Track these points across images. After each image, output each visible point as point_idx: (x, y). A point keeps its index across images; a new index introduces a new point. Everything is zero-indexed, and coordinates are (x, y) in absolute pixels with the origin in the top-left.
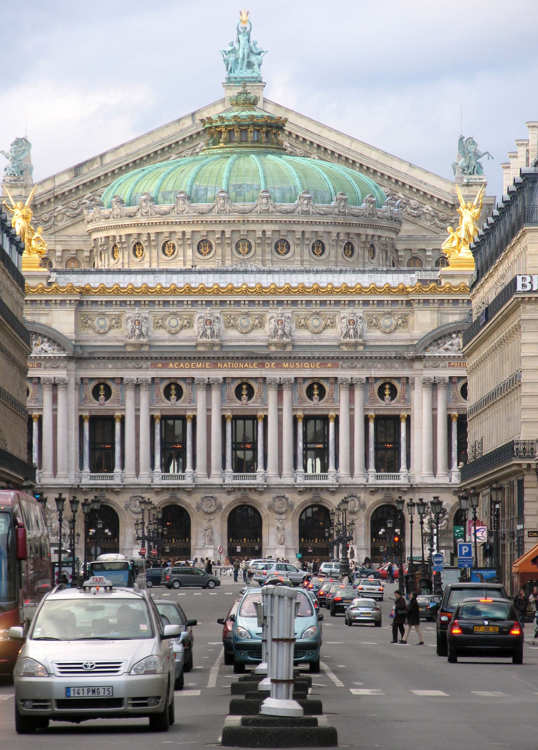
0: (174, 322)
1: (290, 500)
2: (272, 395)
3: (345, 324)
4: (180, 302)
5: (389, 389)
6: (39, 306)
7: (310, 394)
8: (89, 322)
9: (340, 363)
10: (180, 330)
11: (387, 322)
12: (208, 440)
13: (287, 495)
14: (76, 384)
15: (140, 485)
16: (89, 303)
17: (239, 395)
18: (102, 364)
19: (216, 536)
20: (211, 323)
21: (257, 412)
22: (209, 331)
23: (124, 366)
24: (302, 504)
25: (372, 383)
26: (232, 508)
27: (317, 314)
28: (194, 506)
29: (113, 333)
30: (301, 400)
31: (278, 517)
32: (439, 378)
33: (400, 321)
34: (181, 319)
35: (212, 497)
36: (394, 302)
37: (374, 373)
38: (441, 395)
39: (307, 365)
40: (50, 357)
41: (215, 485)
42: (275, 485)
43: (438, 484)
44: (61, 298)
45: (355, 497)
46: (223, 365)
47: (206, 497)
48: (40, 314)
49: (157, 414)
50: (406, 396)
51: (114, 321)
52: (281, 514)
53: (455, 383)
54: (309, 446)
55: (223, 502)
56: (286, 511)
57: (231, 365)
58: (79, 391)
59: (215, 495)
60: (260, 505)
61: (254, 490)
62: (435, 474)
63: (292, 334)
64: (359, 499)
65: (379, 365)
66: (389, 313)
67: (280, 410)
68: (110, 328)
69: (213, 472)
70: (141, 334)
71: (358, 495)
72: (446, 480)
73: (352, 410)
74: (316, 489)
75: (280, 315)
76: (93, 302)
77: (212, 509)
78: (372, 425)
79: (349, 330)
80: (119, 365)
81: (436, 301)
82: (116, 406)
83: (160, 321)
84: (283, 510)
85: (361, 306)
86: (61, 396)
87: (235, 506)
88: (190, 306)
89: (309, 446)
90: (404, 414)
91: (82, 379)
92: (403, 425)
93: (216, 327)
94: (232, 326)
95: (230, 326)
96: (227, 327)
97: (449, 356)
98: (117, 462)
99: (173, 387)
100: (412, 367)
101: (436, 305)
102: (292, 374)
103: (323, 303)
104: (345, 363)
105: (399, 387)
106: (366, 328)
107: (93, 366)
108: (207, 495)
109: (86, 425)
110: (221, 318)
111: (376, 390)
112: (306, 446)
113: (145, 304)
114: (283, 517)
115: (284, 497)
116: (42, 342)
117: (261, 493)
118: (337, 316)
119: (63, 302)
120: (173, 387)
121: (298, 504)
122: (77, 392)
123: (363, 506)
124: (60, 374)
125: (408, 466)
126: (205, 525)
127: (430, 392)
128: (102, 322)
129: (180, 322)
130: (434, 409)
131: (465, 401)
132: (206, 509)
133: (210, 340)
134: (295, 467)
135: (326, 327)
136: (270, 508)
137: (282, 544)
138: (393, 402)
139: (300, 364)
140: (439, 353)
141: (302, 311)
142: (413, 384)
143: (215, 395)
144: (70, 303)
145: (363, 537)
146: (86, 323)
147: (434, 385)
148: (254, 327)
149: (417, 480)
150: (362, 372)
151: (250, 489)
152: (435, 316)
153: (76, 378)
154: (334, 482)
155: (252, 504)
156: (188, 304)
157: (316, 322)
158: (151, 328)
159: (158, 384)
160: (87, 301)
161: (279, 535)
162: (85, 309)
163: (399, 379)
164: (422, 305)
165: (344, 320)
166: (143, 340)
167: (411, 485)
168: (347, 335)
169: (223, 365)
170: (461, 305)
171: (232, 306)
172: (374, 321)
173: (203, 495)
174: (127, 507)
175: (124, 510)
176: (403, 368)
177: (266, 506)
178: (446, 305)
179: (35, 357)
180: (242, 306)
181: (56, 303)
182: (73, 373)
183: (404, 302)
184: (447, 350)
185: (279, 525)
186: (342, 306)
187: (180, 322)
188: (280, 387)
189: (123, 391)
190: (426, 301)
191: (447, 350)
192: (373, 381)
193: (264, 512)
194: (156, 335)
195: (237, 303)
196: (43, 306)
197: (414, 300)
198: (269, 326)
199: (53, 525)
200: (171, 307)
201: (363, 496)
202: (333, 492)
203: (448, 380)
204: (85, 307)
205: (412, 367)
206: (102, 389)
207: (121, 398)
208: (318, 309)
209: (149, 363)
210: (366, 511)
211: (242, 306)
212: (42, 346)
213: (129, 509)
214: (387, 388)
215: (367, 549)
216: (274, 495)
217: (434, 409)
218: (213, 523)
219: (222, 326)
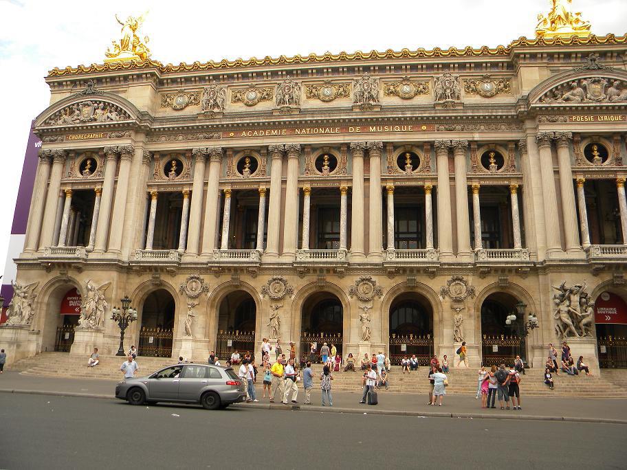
0: (252, 95)
1: (377, 284)
2: (358, 162)
3: (440, 86)
4: (260, 74)
5: (494, 158)
6: (118, 84)
7: (402, 165)
8: (168, 100)
9: (436, 126)
10: (259, 102)
11: (487, 86)
12: (284, 218)
13: (374, 278)
14: (144, 157)
15: (198, 264)
16: (169, 81)
17: (319, 166)
18: (172, 137)
19: (285, 329)
20: (289, 89)
21: (340, 184)
22: (287, 96)
23: (195, 137)
24: (393, 290)
25: (474, 151)
26: (306, 295)
27: (406, 79)
28: (259, 290)
29: (188, 109)
30: (390, 169)
31: (362, 305)
32: (560, 134)
33: (502, 85)
34: (260, 92)
35: (281, 280)
36: (495, 65)
37: (477, 137)
38: (564, 154)
39: (397, 128)
40: (114, 125)
41: (285, 264)
42: (359, 265)
43: (572, 260)
44: (137, 73)
45: (461, 280)
46: (301, 132)
47: (274, 280)
48: (118, 92)
49: (227, 188)
50: (515, 164)
51: (192, 98)
52: (366, 301)
53: (577, 143)
54: (401, 236)
55: (295, 285)
56: (373, 297)
57: (310, 131)
58: (150, 167)
59: (285, 278)
60: (340, 290)
61: (332, 271)
62: (565, 248)
63: (380, 100)
64: (466, 283)
65: (482, 127)
66: (488, 77)
67: (367, 180)
68: (187, 105)
69: (285, 250)
70: (216, 105)
71: (465, 278)
72: (583, 256)
73: (452, 179)
74: (412, 269)
75: (367, 78)
76: (174, 81)
77: (280, 295)
78: (476, 197)
79: (445, 90)
80: (190, 137)
81: (545, 55)
82: (184, 181)
83: (238, 95)
84: (370, 295)
85: (457, 71)
86: (124, 165)
87: (310, 292)
88: (270, 79)
89: (401, 236)
90: (514, 184)
91: (153, 154)
92: (514, 197)
93: (296, 93)
94: (314, 96)
95: (312, 95)
96: (308, 98)
97: (571, 107)
98: (182, 242)
99: (248, 160)
100: (522, 128)
101: (544, 61)
102: (381, 139)
103: (414, 67)
104: (441, 124)
105: (506, 155)
106: (463, 93)
107: (163, 139)
108: (275, 277)
109: (154, 202)
110: (302, 89)
111: (479, 158)
112: (398, 236)
113: (224, 79)
114: (369, 305)
115: (369, 280)
116: (111, 112)
117: (341, 275)
118: (430, 82)
119: (139, 76)
120: (248, 160)
121: (388, 289)
122: (145, 166)
123: (471, 292)
124: (124, 143)
125: (524, 244)
126: (271, 312)
127: (549, 150)
128: (180, 100)
129: (259, 95)
130: (557, 172)
131: (591, 164)
132: (274, 295)
133: (288, 105)
134: (385, 246)
135: (418, 93)
136: (352, 293)
137: (366, 340)
138: (500, 170)
139: (389, 128)
140: (559, 103)
141: (390, 76)
142: (525, 146)
143: (293, 163)
144: (147, 78)
145: (473, 332)
146: (166, 101)
147: (554, 143)
148: (338, 96)
149: (541, 259)
150: (462, 135)
151: (328, 270)
152: (546, 74)
153: (144, 152)
154: (435, 260)
155: (331, 290)
156: (267, 76)
157: (406, 89)
158: (229, 102)
159: (230, 156)
160: (167, 79)
161: (364, 329)
162: (166, 88)
163: (504, 144)
164: (527, 61)
165: (439, 82)
166: (216, 110)
167: (534, 263)
168: (443, 96)
169: (301, 132)
170: (573, 61)
171: (315, 76)
172: (472, 85)
173: (270, 278)
174: (183, 290)
175: (179, 294)
176: (512, 131)
177: (347, 291)
178: (556, 61)
179: (100, 126)
180: (325, 76)
181: (133, 79)
182: (141, 144)
183: (505, 64)
184: (567, 100)
185: (364, 315)
186: (436, 71)
187: (259, 95)
188: (367, 153)
189: (193, 165)
190: (534, 56)
191: (567, 100)
192: (476, 147)
193: (347, 299)
194: (233, 108)
195: (320, 71)
196: (122, 83)
197: (517, 56)
198: (354, 91)
199: (88, 306)
200: (251, 80)
201: (471, 280)
202: (431, 272)
203: (570, 136)
204: (166, 86)
205: (522, 128)
206: (174, 163)
207: (191, 173)
208: (409, 74)
209: (221, 133)
210: (474, 299)
211: (325, 76)
212: (109, 114)
213: (184, 292)
214: (491, 154)
215: (477, 347)
216: (358, 278)
217: (557, 172)
218: (280, 313)
219: (303, 97)
